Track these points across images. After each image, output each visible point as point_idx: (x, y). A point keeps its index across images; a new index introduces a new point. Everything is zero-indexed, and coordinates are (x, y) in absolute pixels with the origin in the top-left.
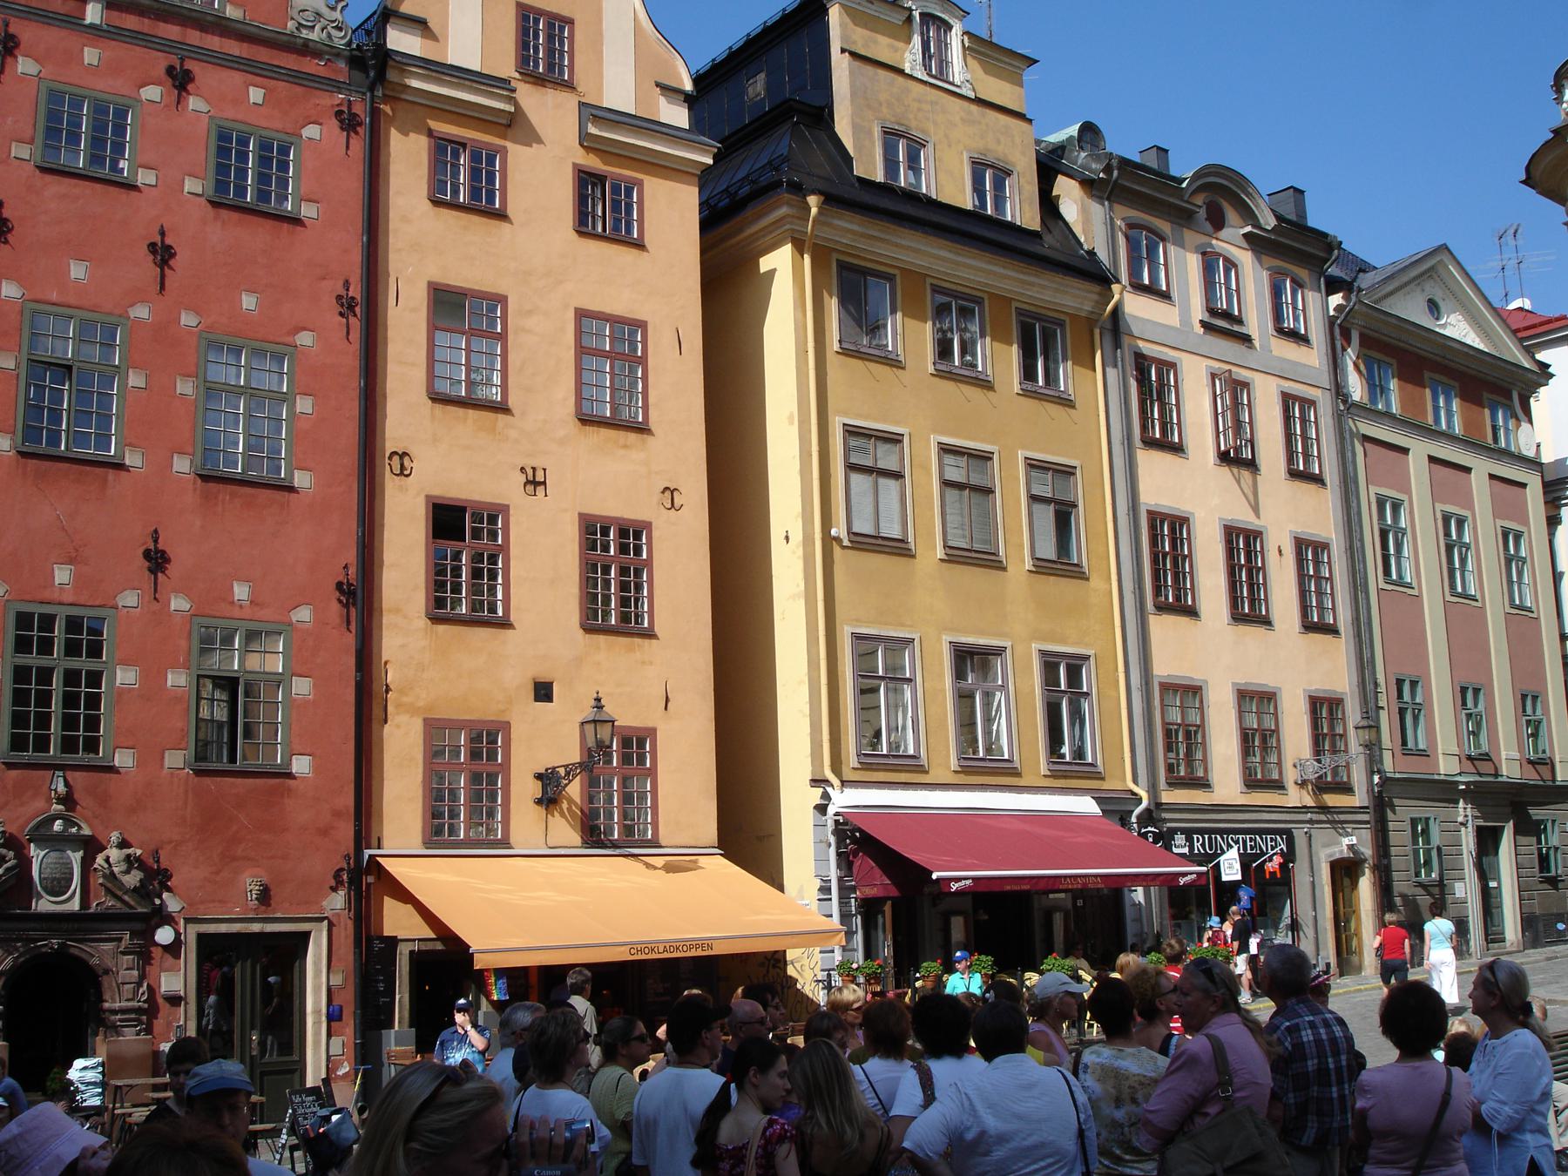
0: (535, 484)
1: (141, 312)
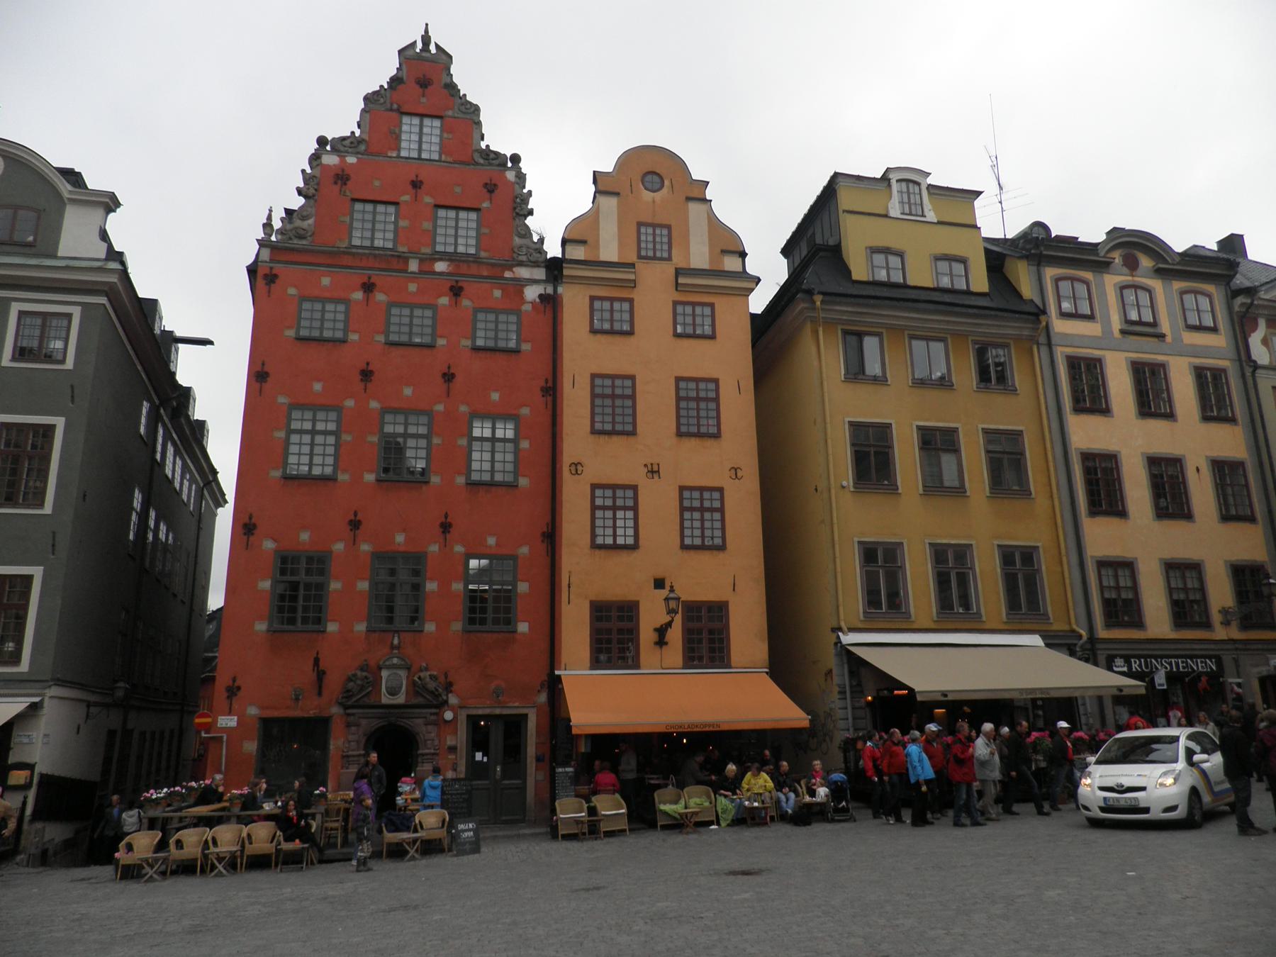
0: (652, 472)
1: (440, 408)
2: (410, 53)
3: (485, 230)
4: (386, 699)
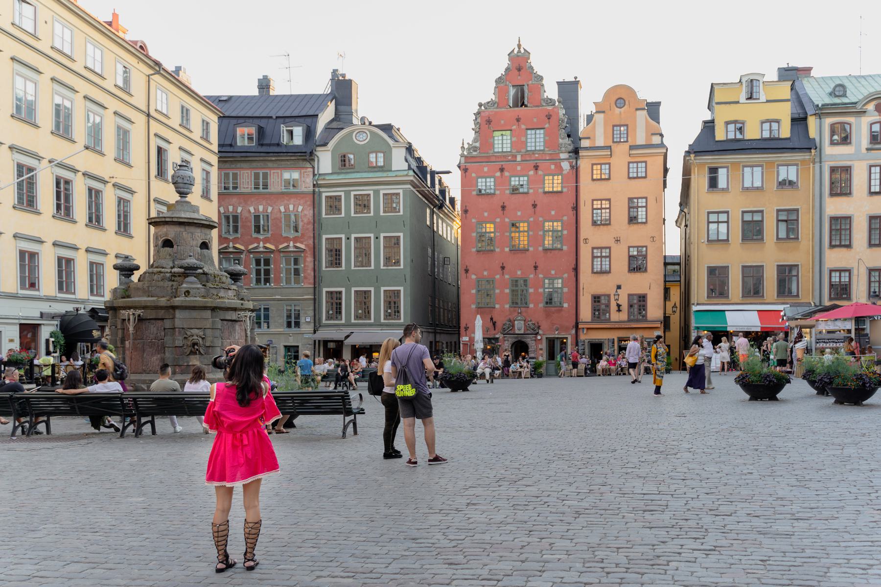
1: (532, 219)
4: (517, 332)
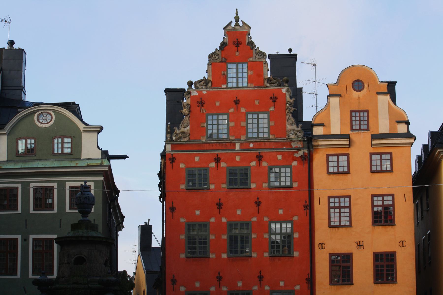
0: (360, 246)
1: (254, 219)
2: (229, 28)
3: (272, 124)
